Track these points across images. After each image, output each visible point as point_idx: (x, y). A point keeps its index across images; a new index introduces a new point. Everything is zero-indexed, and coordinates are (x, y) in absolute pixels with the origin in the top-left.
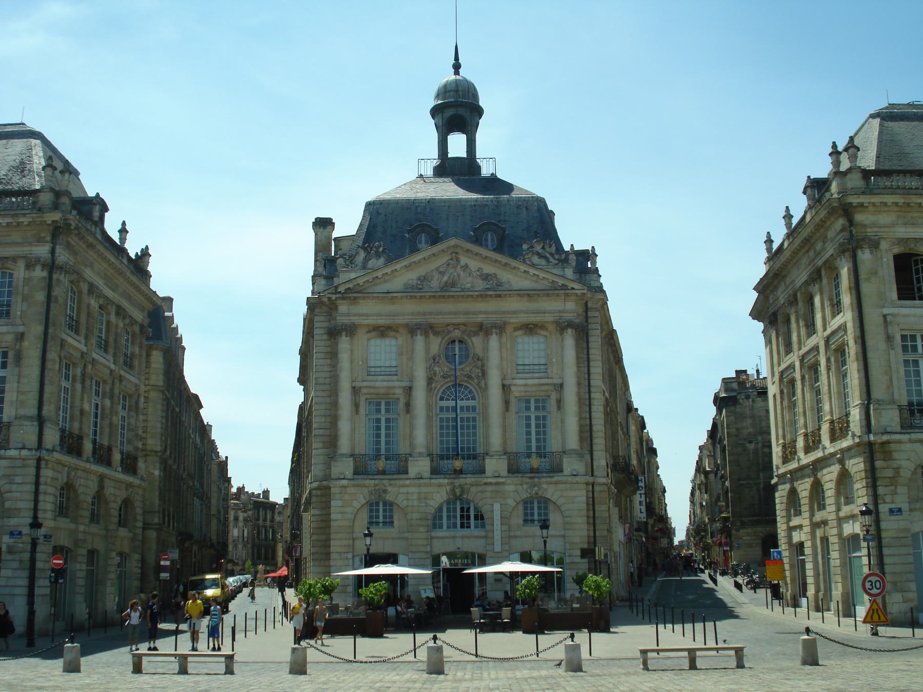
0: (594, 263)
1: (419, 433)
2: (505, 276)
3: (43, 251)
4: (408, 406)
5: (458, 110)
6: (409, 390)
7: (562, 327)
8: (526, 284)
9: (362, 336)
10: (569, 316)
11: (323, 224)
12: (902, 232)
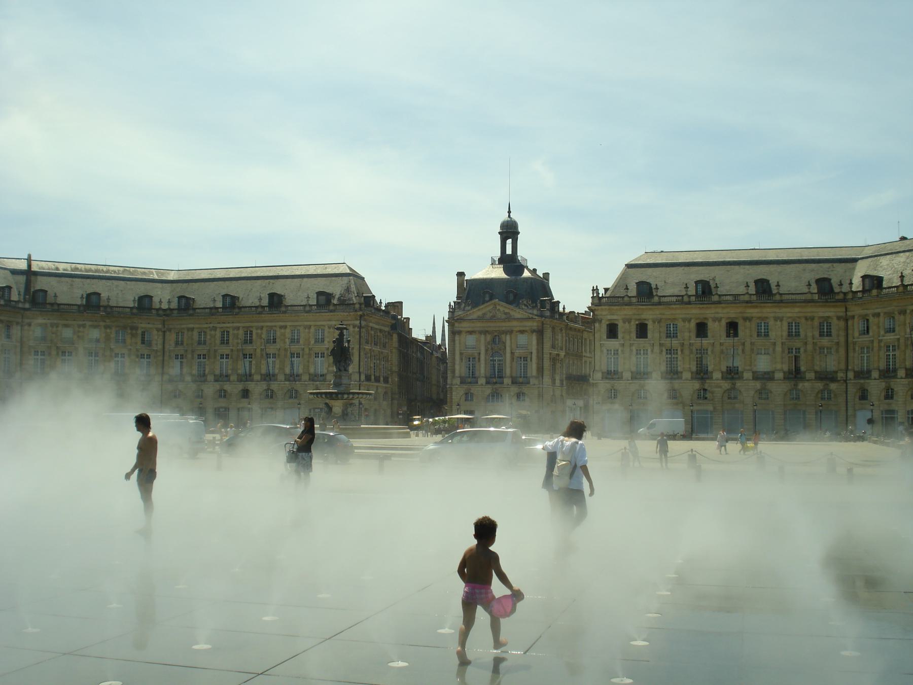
1: (482, 369)
2: (512, 313)
3: (358, 322)
5: (509, 231)
7: (533, 331)
8: (519, 316)
9: (463, 335)
10: (535, 328)
11: (461, 275)
12: (609, 317)
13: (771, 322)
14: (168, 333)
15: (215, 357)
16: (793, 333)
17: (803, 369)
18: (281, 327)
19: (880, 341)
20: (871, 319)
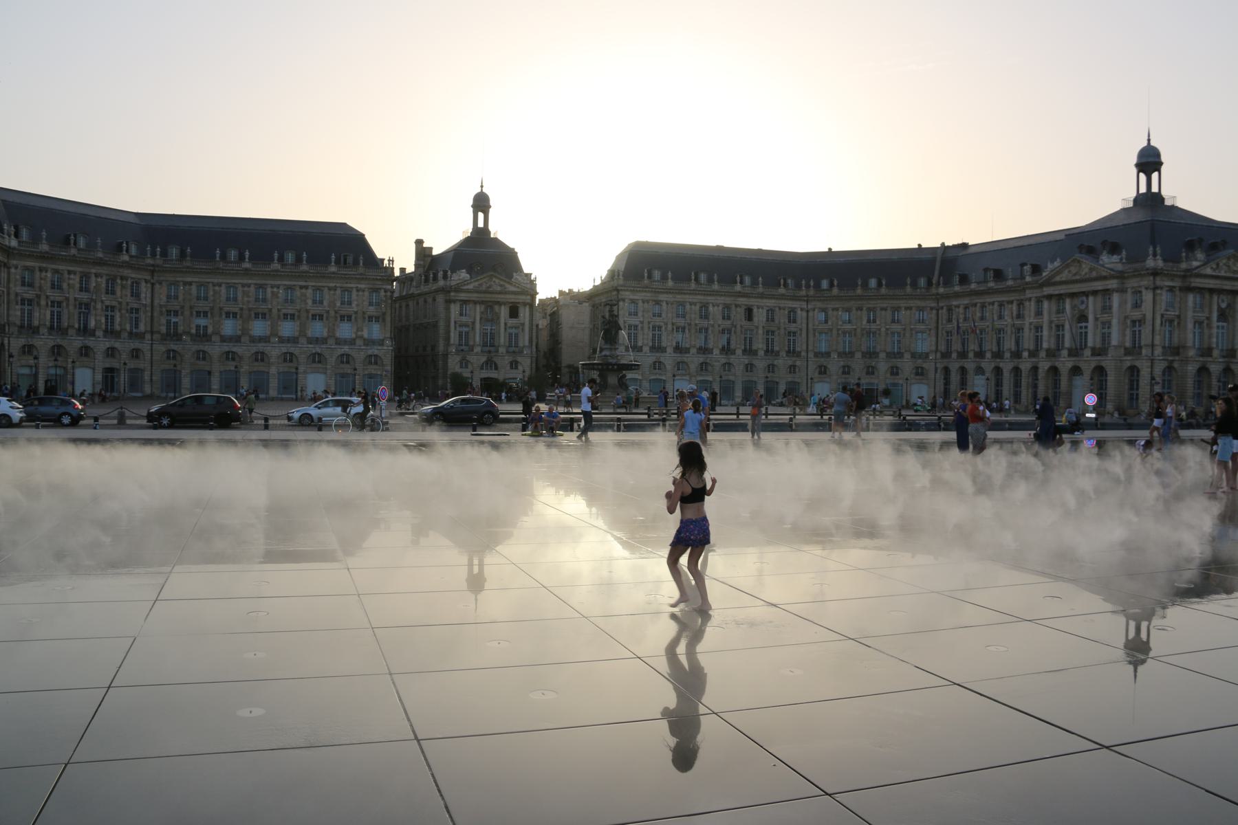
2: (507, 286)
4: (473, 328)
5: (481, 203)
6: (474, 323)
13: (755, 310)
14: (157, 286)
15: (221, 315)
16: (771, 317)
17: (776, 348)
18: (301, 287)
20: (830, 312)
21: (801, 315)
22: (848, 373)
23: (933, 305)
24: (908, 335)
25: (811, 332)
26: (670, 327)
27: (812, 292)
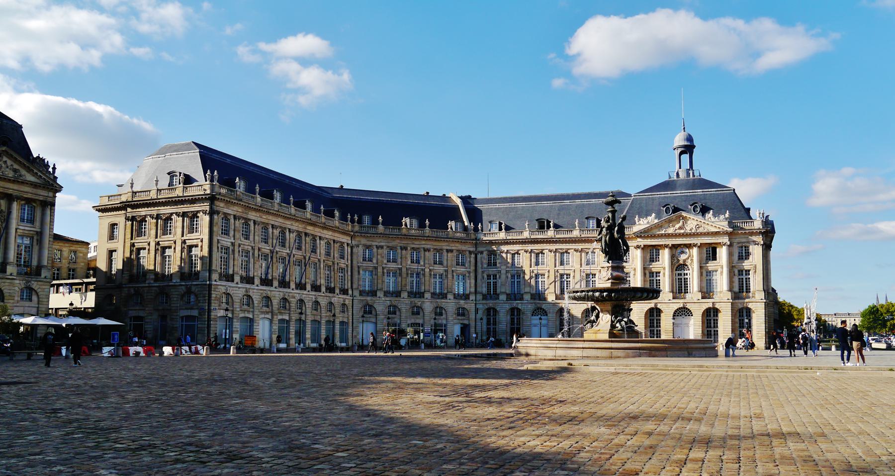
0: (54, 172)
12: (226, 210)
13: (318, 241)
19: (383, 268)
21: (347, 250)
22: (394, 313)
23: (472, 249)
24: (450, 276)
25: (356, 269)
26: (256, 252)
27: (357, 228)
